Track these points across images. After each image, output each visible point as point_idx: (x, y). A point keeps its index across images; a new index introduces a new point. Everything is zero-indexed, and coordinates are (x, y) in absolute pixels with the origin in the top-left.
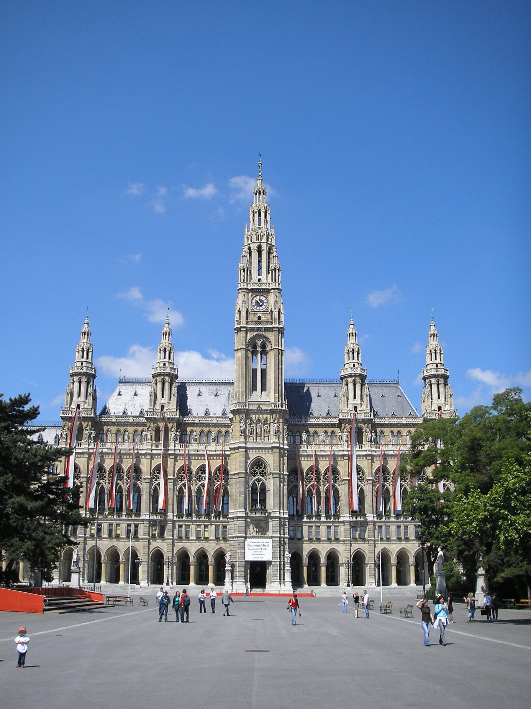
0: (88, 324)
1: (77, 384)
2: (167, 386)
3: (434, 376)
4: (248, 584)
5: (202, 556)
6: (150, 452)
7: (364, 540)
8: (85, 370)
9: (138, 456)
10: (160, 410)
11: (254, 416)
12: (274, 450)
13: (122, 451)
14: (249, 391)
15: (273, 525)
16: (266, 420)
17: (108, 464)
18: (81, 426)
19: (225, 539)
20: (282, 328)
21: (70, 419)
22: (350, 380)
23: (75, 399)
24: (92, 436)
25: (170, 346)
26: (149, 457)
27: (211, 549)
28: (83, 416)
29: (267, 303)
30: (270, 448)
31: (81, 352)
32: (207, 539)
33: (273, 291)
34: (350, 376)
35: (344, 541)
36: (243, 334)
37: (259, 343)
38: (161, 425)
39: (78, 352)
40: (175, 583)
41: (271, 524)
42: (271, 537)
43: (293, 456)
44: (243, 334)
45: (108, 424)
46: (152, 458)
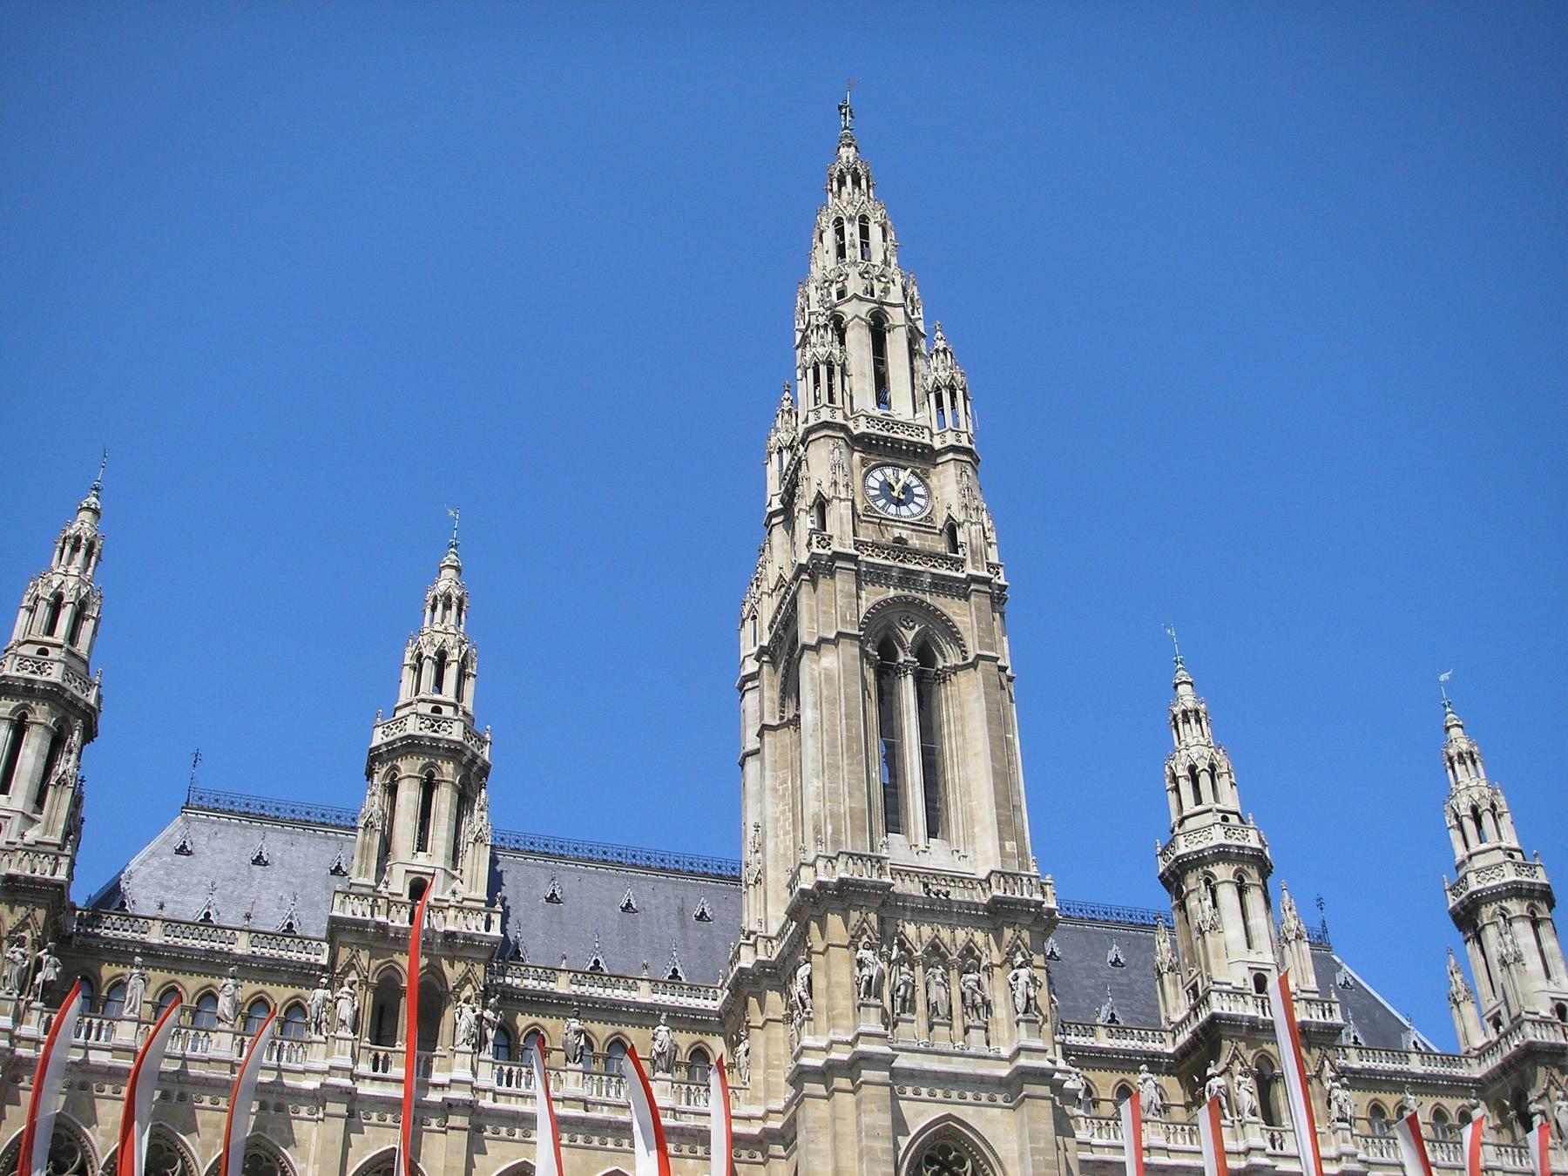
0: (96, 512)
2: (444, 800)
6: (347, 1082)
9: (277, 1102)
10: (406, 898)
11: (910, 930)
12: (1029, 1089)
13: (195, 1070)
14: (880, 826)
16: (969, 950)
20: (1003, 588)
22: (1223, 872)
24: (40, 977)
25: (464, 648)
26: (342, 1109)
28: (13, 870)
29: (929, 495)
30: (1000, 1083)
31: (43, 610)
33: (951, 456)
36: (843, 582)
37: (910, 636)
39: (32, 610)
44: (843, 582)
45: (121, 953)
46: (353, 1123)
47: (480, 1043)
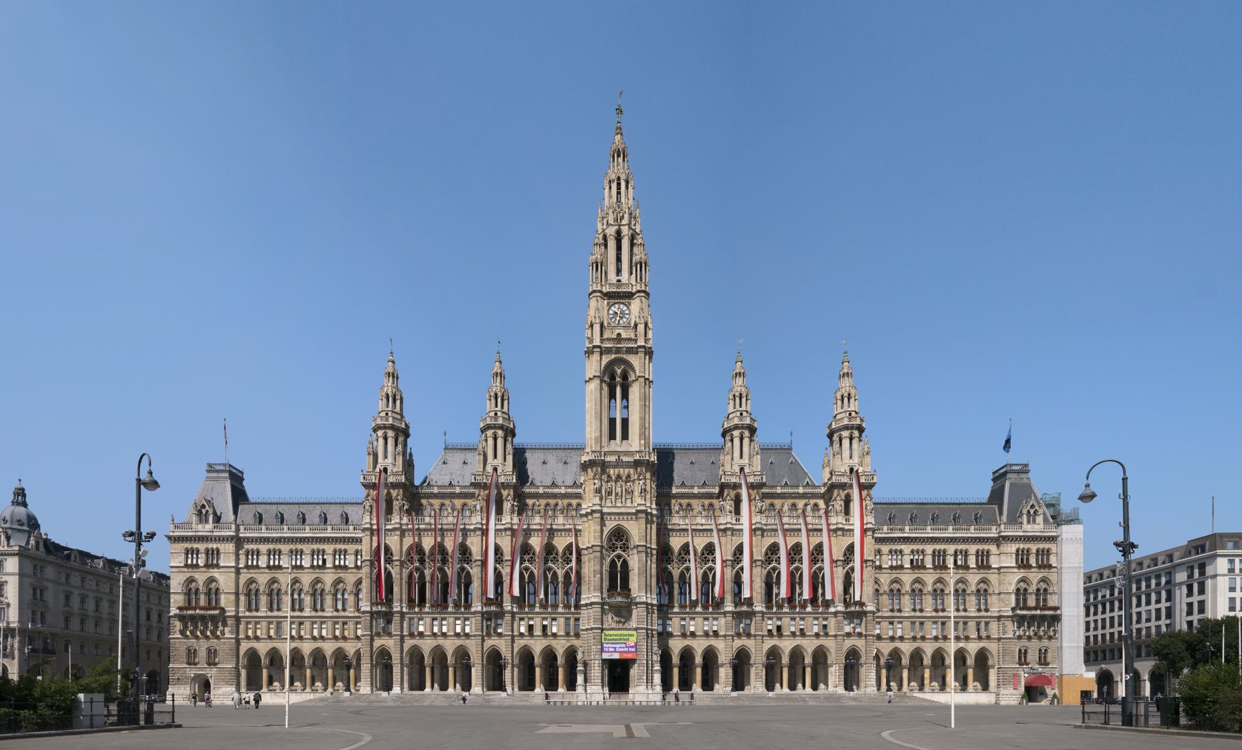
1: (381, 441)
2: (500, 442)
3: (846, 428)
4: (606, 690)
5: (550, 655)
7: (749, 635)
8: (391, 421)
15: (638, 614)
17: (428, 543)
18: (389, 494)
19: (577, 635)
21: (374, 486)
22: (736, 433)
23: (380, 460)
27: (560, 647)
32: (554, 635)
34: (736, 427)
35: (725, 636)
38: (494, 492)
40: (516, 689)
41: (635, 612)
42: (636, 629)
43: (663, 533)
47: (513, 512)
